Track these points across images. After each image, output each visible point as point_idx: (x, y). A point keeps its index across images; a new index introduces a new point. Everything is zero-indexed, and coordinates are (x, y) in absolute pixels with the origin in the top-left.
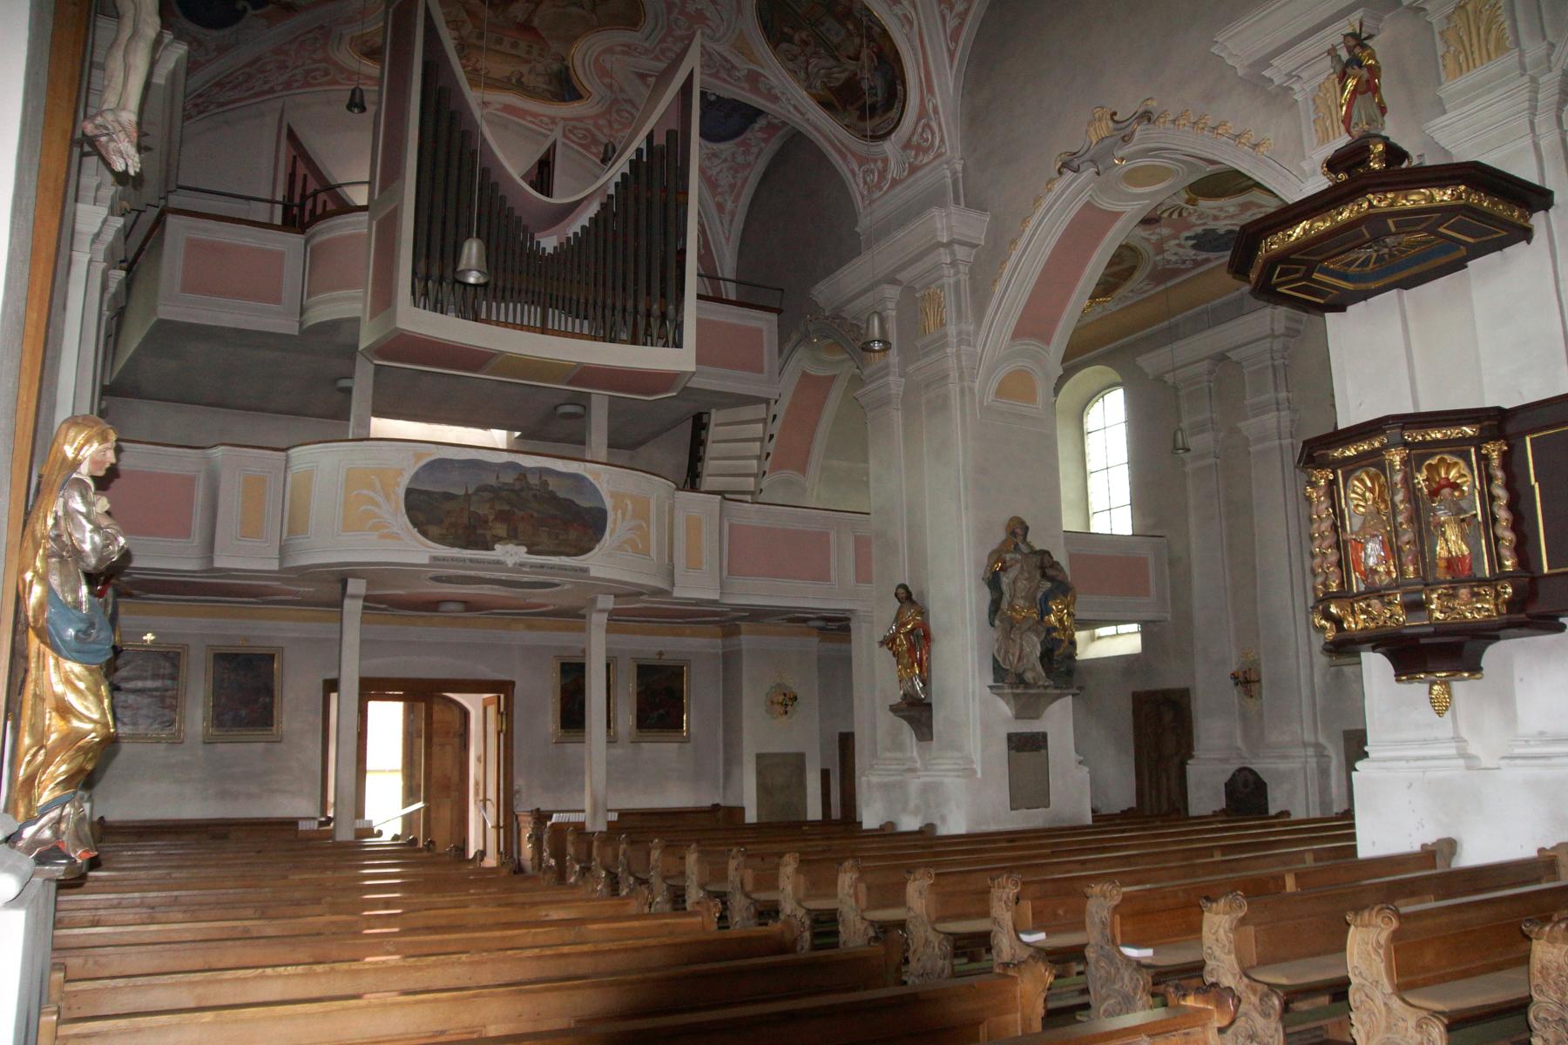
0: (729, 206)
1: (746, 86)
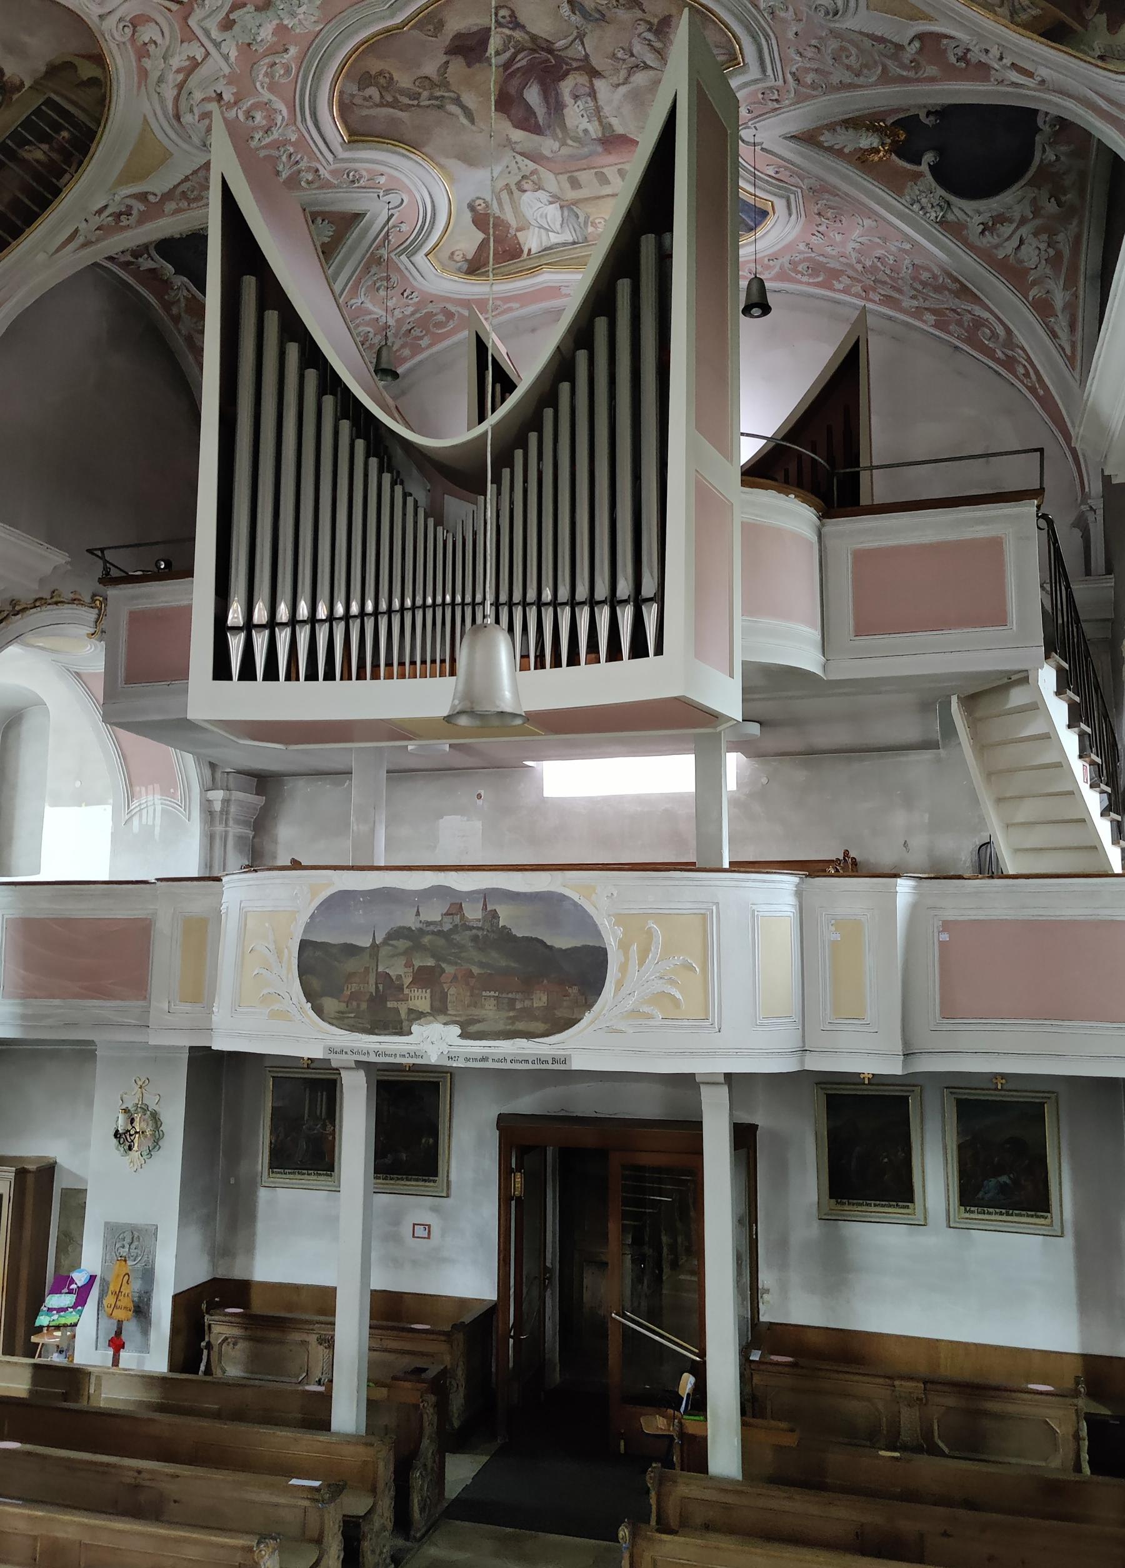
0: (1059, 298)
1: (931, 70)
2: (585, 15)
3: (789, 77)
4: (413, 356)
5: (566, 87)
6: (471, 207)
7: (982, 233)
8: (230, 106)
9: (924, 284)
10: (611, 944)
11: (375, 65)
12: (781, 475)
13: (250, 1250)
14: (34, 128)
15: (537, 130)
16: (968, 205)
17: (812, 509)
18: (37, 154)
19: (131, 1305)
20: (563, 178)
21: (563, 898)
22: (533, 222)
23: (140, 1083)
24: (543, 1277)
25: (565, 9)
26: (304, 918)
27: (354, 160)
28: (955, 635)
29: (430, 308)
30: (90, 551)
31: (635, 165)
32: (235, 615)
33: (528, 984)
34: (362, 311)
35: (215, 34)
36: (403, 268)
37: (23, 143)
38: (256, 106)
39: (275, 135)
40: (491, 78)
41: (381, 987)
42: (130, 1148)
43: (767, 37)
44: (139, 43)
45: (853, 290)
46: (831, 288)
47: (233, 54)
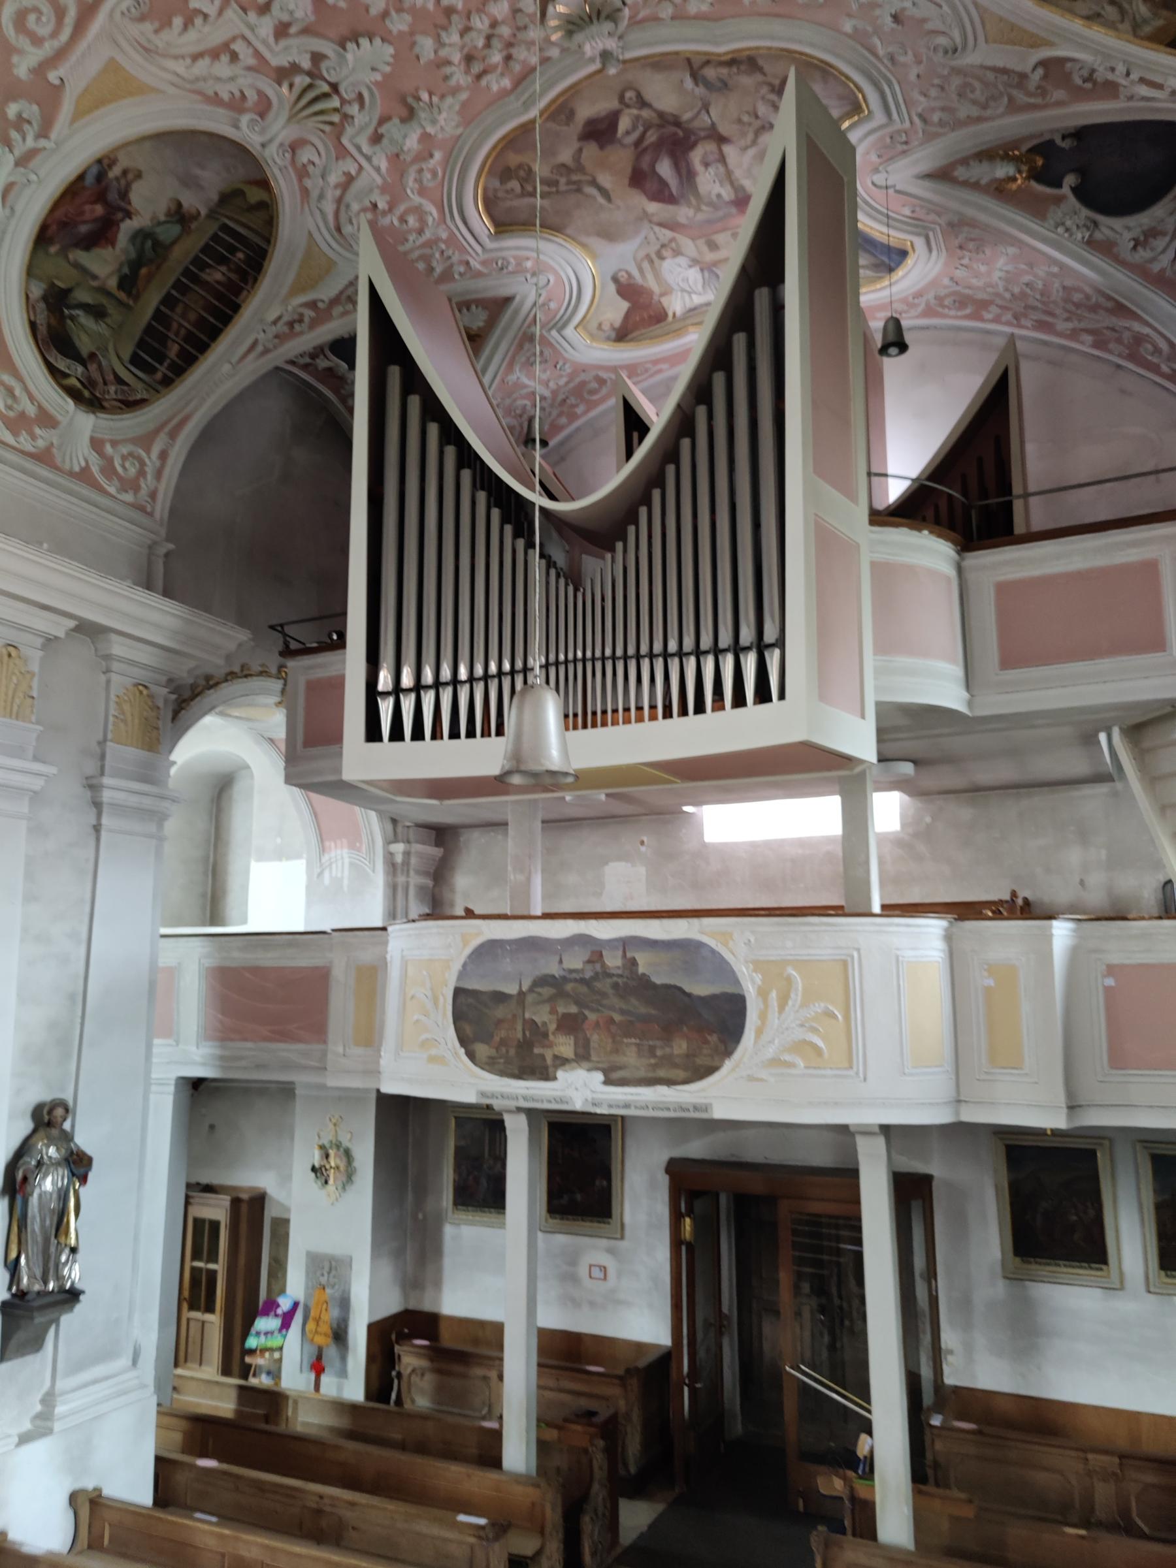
1: (1059, 94)
2: (708, 85)
3: (916, 120)
4: (571, 421)
5: (696, 157)
6: (615, 279)
7: (1135, 248)
8: (384, 213)
9: (1078, 305)
10: (750, 991)
11: (513, 159)
12: (930, 514)
13: (438, 1284)
14: (213, 252)
15: (671, 200)
16: (1117, 223)
17: (950, 544)
18: (216, 275)
19: (329, 1332)
20: (701, 242)
21: (700, 945)
22: (676, 287)
23: (334, 1121)
24: (719, 1324)
25: (689, 83)
26: (457, 966)
27: (501, 249)
28: (1105, 664)
29: (583, 377)
30: (272, 627)
31: (748, 223)
32: (385, 680)
33: (668, 1031)
34: (518, 385)
35: (366, 149)
36: (552, 341)
37: (203, 266)
38: (407, 211)
39: (428, 235)
40: (621, 157)
41: (528, 1033)
42: (326, 1182)
43: (890, 85)
44: (299, 165)
45: (1004, 319)
46: (982, 320)
47: (384, 166)
